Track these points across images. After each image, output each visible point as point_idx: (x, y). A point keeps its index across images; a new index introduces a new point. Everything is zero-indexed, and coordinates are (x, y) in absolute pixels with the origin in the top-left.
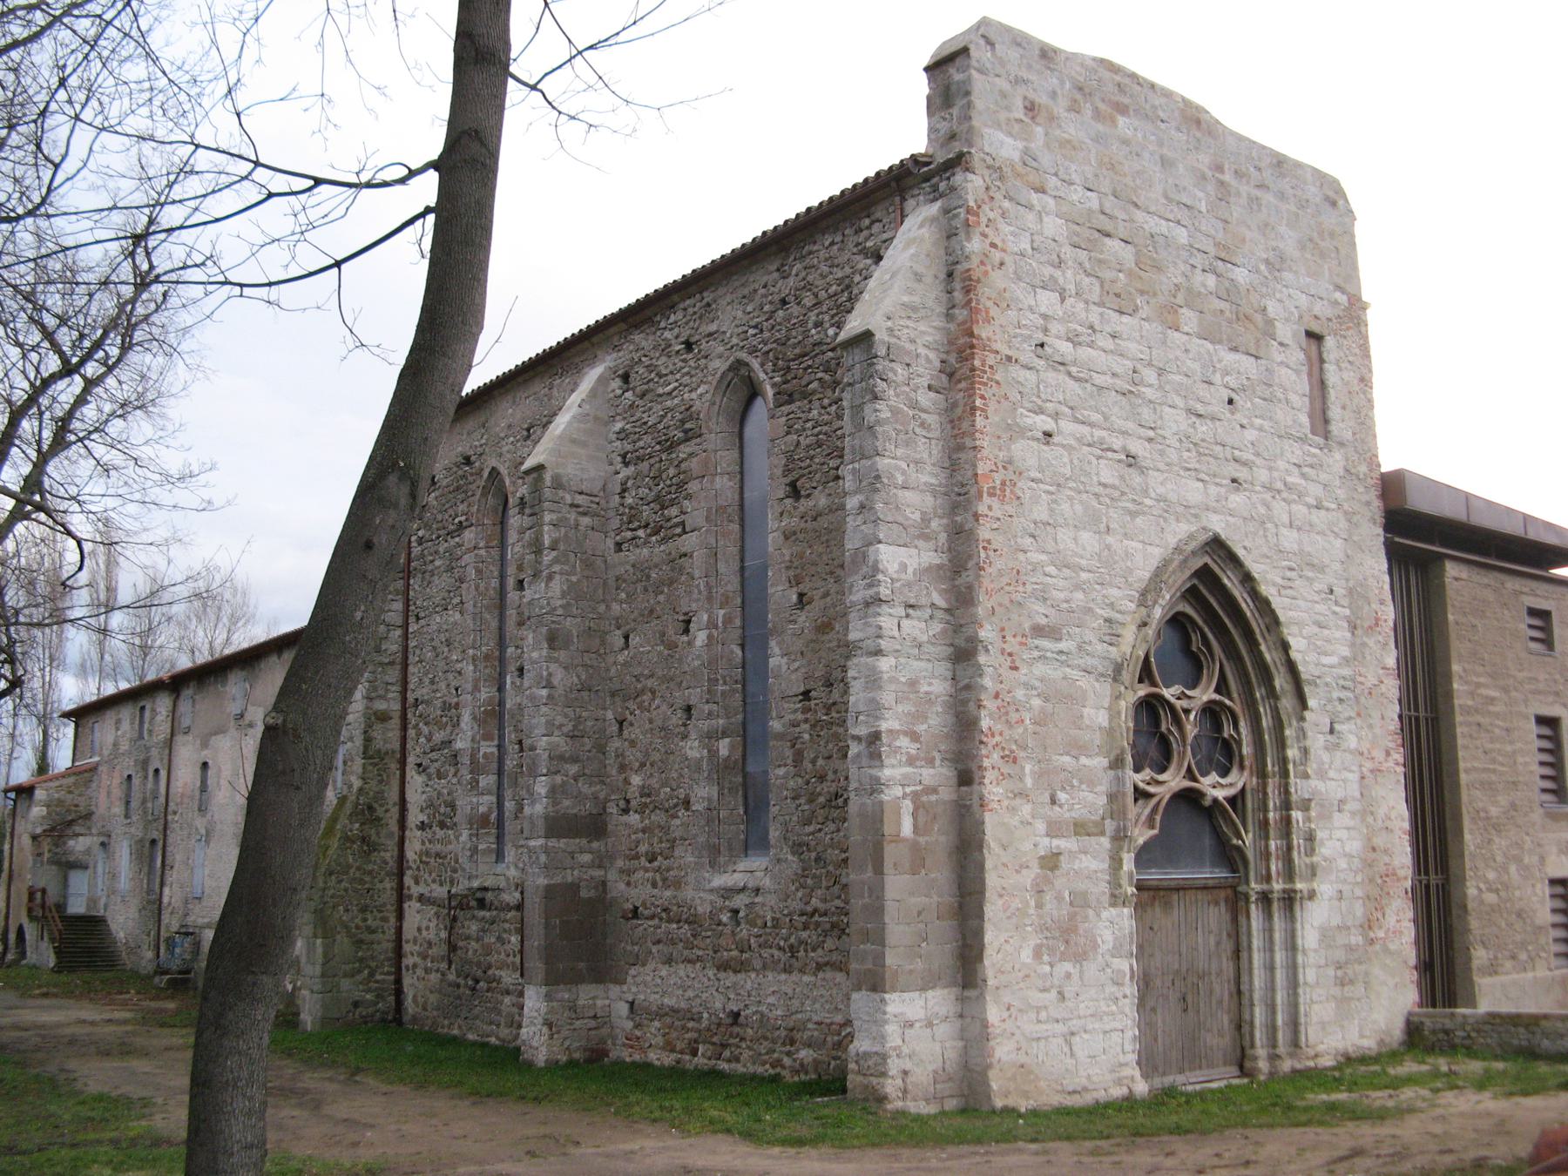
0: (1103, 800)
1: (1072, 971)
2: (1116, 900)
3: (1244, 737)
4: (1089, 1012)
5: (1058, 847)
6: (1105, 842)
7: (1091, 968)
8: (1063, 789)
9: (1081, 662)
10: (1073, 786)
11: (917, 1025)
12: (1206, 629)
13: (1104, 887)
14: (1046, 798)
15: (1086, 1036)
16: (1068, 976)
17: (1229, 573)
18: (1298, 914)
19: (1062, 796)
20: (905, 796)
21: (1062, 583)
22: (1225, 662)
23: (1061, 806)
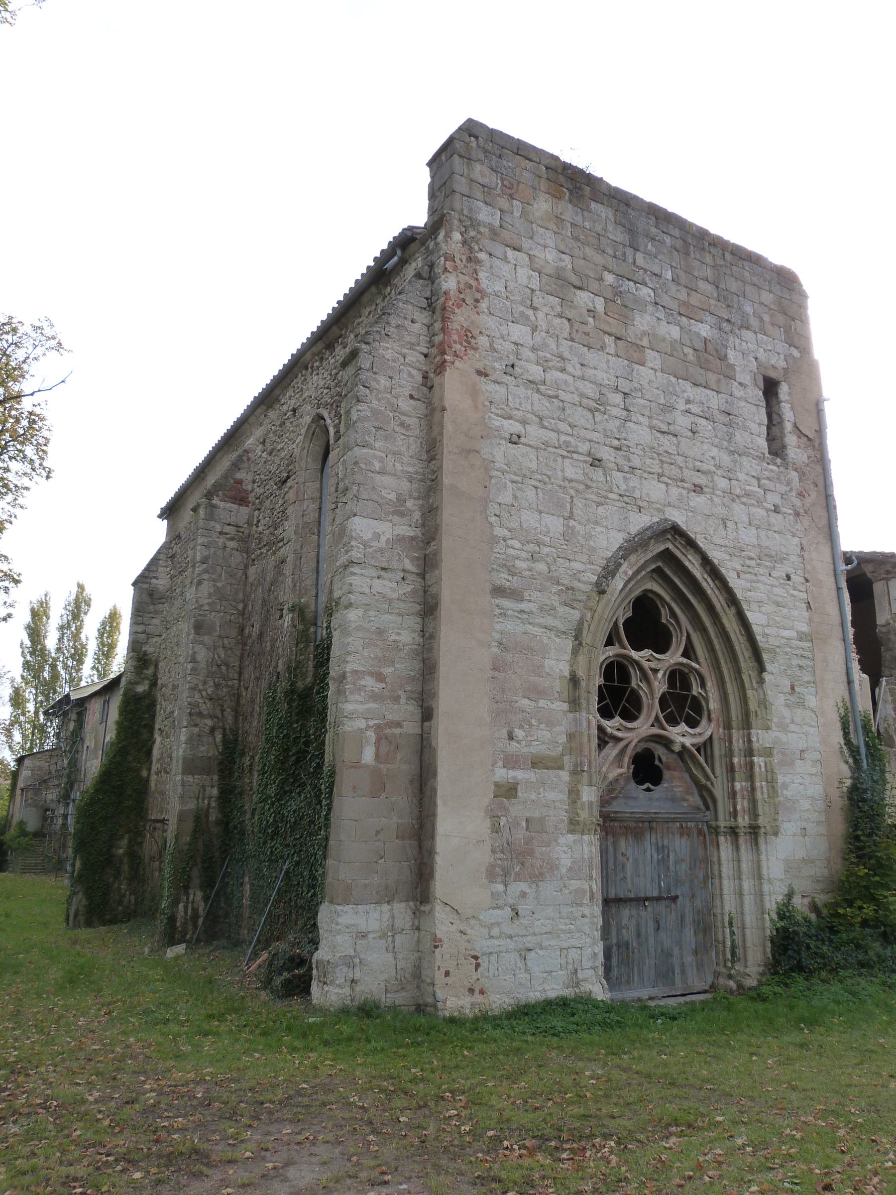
0: (563, 739)
2: (574, 825)
3: (710, 695)
4: (545, 930)
5: (515, 778)
6: (565, 776)
7: (548, 888)
8: (521, 727)
9: (541, 621)
10: (531, 725)
11: (371, 936)
12: (674, 605)
13: (564, 816)
14: (504, 733)
15: (541, 952)
16: (523, 895)
17: (689, 557)
18: (762, 847)
19: (519, 733)
20: (368, 727)
21: (524, 555)
22: (691, 631)
23: (518, 742)
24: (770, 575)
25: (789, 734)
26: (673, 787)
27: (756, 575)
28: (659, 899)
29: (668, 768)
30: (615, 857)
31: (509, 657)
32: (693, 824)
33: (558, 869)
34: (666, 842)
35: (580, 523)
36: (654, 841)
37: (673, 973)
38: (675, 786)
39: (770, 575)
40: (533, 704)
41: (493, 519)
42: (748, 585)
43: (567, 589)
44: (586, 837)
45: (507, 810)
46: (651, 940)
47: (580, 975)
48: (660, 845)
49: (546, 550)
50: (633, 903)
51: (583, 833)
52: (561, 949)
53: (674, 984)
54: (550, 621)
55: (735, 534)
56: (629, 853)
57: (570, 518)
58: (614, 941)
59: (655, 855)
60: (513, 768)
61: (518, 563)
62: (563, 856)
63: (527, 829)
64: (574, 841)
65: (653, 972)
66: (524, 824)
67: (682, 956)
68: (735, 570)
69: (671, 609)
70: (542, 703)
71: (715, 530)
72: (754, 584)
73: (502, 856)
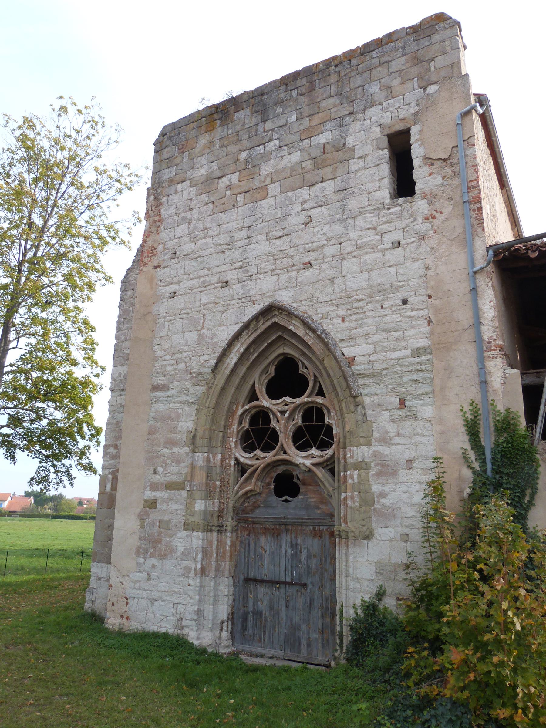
1: (156, 564)
2: (187, 526)
4: (164, 589)
5: (155, 496)
6: (184, 494)
7: (169, 564)
8: (161, 466)
10: (167, 464)
11: (103, 579)
14: (152, 470)
15: (162, 603)
16: (154, 566)
18: (351, 548)
19: (160, 470)
20: (109, 473)
23: (160, 475)
24: (382, 307)
25: (393, 447)
26: (307, 498)
27: (365, 312)
28: (290, 584)
29: (304, 484)
30: (256, 549)
31: (158, 425)
32: (325, 528)
33: (175, 553)
34: (299, 541)
35: (208, 330)
36: (289, 539)
37: (300, 644)
38: (311, 498)
39: (382, 307)
40: (169, 451)
41: (155, 348)
42: (354, 325)
43: (198, 374)
44: (195, 534)
45: (149, 515)
46: (283, 614)
47: (184, 623)
48: (294, 543)
49: (185, 355)
50: (268, 585)
51: (193, 530)
52: (174, 604)
53: (299, 652)
54: (184, 398)
55: (343, 287)
56: (268, 548)
57: (202, 329)
58: (251, 609)
59: (289, 551)
60: (155, 491)
61: (169, 368)
62: (180, 544)
63: (159, 527)
64: (187, 536)
65: (282, 638)
66: (158, 524)
67: (308, 633)
68: (340, 316)
69: (302, 362)
70: (175, 450)
71: (321, 292)
72: (360, 322)
73: (145, 542)
